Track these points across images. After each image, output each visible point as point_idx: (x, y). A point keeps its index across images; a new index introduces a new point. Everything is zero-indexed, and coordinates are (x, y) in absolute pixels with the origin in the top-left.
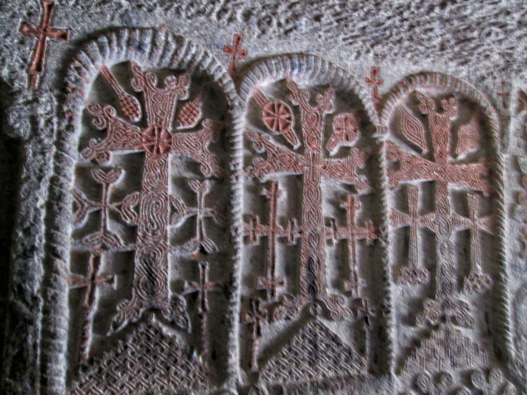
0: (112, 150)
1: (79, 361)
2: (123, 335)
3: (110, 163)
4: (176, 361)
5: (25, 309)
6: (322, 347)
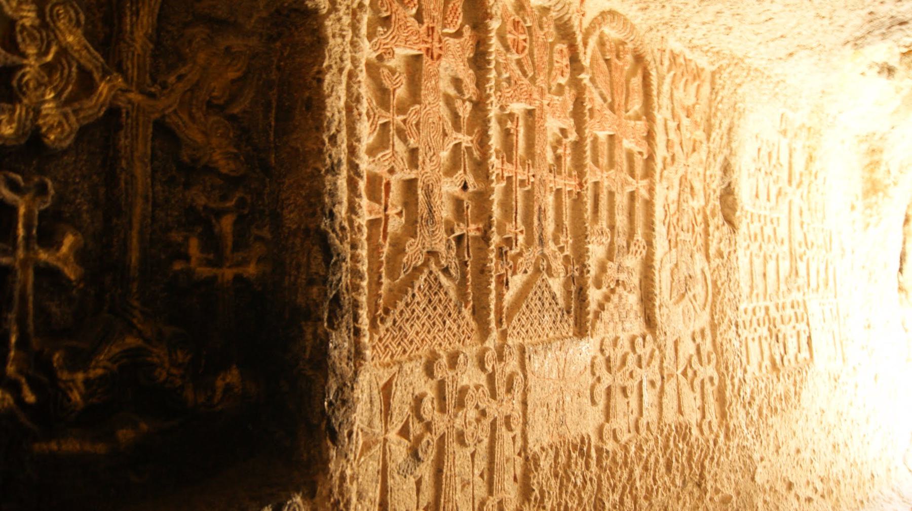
0: (397, 46)
1: (377, 311)
2: (410, 281)
3: (392, 63)
4: (450, 315)
5: (337, 242)
6: (547, 305)
